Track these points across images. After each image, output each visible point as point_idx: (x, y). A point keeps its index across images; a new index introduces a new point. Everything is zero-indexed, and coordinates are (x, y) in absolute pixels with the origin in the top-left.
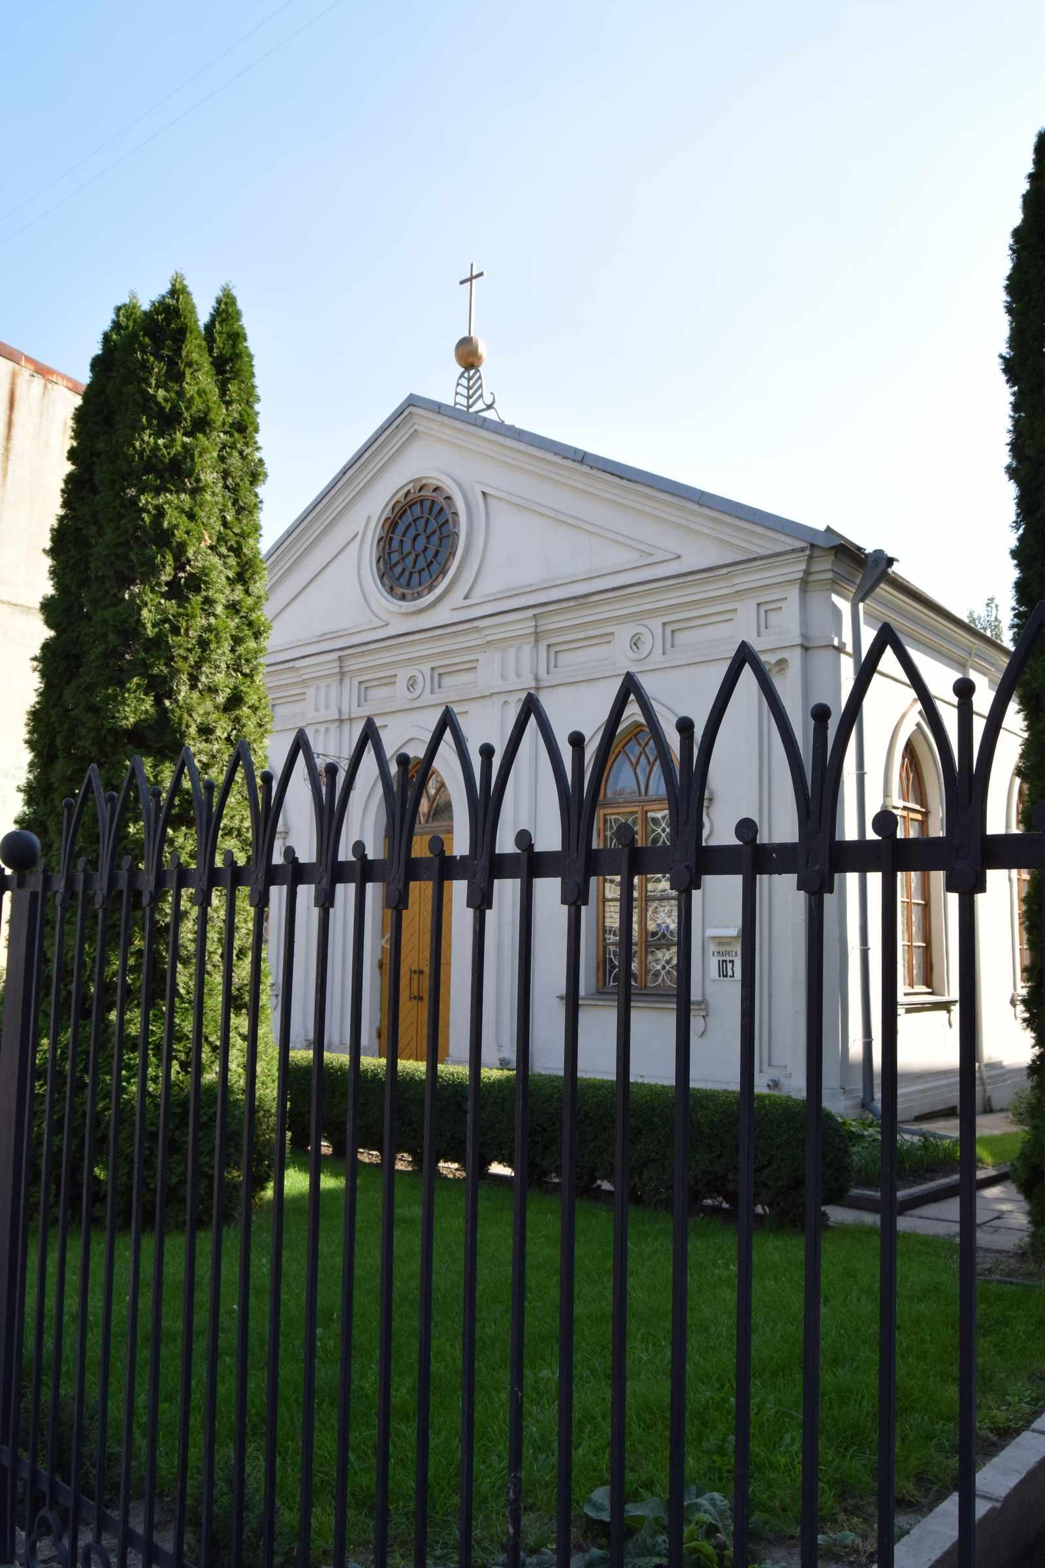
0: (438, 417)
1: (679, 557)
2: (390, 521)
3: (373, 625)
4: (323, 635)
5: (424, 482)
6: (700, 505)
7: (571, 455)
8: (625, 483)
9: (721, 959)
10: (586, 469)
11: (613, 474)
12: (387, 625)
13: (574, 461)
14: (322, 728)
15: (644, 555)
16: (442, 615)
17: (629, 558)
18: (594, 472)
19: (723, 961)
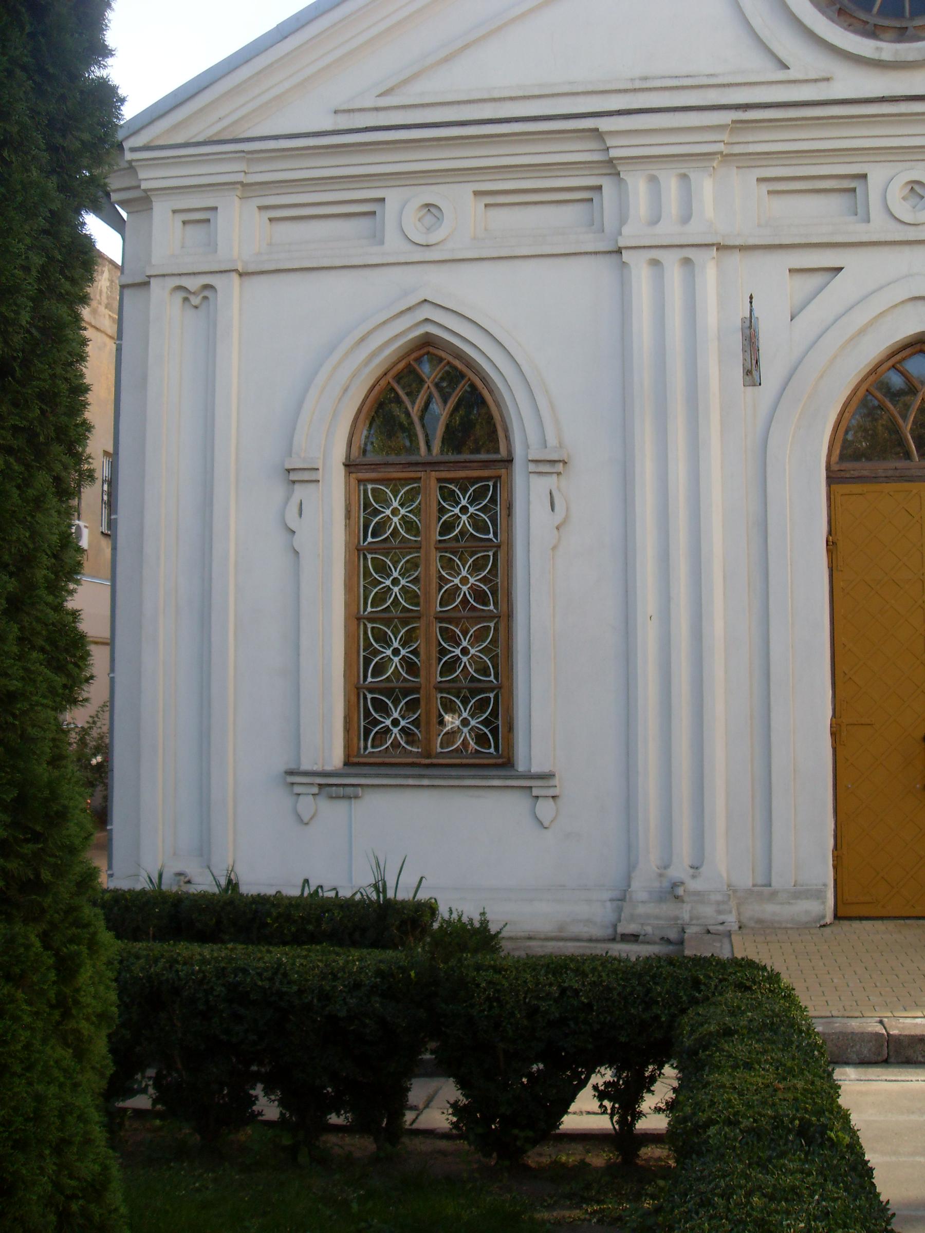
3: (792, 74)
4: (645, 79)
14: (671, 260)
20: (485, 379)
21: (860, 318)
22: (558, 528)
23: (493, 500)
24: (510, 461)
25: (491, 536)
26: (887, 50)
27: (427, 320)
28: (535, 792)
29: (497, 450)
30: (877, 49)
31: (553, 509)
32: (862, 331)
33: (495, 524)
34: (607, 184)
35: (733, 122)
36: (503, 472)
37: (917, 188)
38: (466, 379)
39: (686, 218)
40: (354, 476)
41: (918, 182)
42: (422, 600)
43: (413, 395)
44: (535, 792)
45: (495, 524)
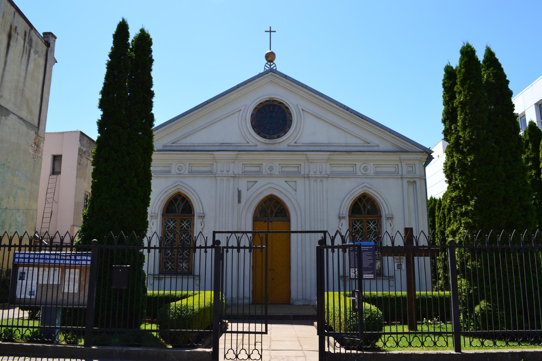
0: (285, 80)
1: (379, 146)
2: (257, 109)
3: (250, 144)
4: (222, 143)
5: (274, 99)
6: (390, 133)
7: (343, 107)
8: (363, 120)
9: (398, 264)
10: (348, 112)
11: (359, 117)
12: (256, 146)
13: (344, 109)
14: (225, 179)
15: (366, 143)
16: (283, 146)
17: (360, 142)
18: (352, 114)
19: (398, 264)
20: (189, 199)
21: (260, 191)
22: (202, 229)
23: (191, 223)
24: (194, 215)
25: (190, 230)
26: (267, 141)
27: (179, 188)
28: (196, 279)
29: (192, 213)
30: (265, 140)
31: (201, 225)
32: (260, 193)
33: (191, 227)
34: (215, 164)
35: (238, 154)
36: (193, 217)
37: (272, 167)
38: (186, 200)
39: (228, 171)
40: (164, 217)
41: (272, 166)
42: (176, 242)
43: (176, 202)
44: (196, 279)
45: (191, 227)
